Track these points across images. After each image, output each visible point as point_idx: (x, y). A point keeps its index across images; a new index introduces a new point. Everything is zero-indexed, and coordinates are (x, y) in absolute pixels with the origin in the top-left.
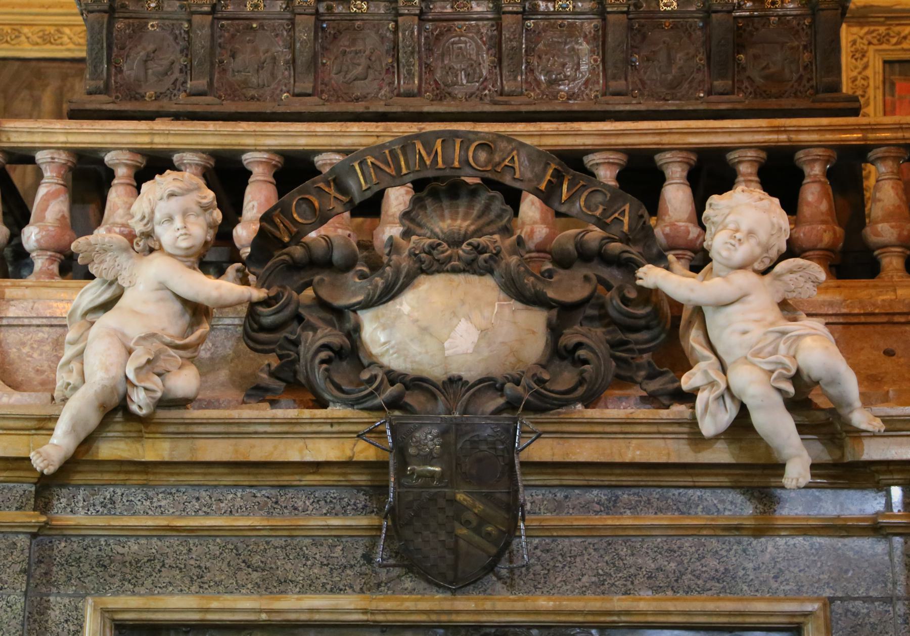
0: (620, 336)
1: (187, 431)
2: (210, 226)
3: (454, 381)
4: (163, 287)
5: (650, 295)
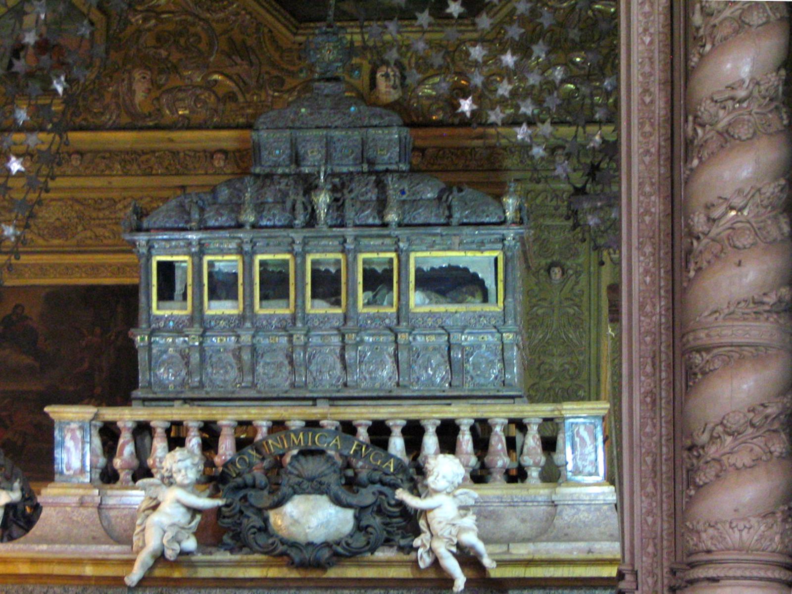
0: (388, 520)
1: (193, 565)
2: (199, 471)
3: (310, 544)
4: (178, 501)
5: (401, 504)
